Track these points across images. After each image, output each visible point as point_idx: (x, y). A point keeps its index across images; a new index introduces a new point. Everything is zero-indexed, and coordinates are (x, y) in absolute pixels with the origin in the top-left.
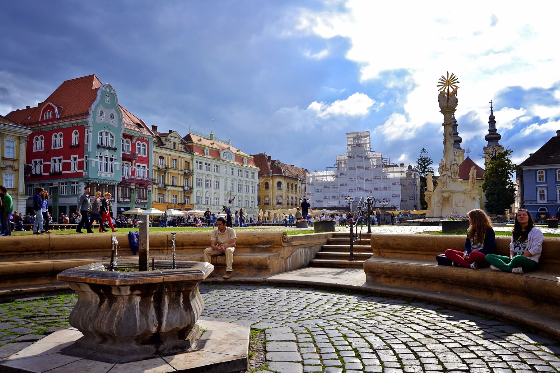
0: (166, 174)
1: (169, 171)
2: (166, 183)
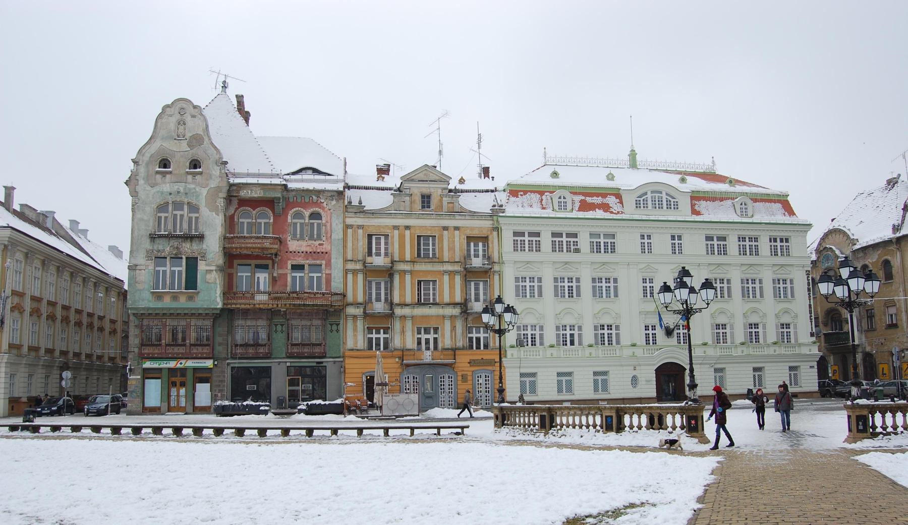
0: (397, 278)
1: (457, 268)
2: (396, 300)
